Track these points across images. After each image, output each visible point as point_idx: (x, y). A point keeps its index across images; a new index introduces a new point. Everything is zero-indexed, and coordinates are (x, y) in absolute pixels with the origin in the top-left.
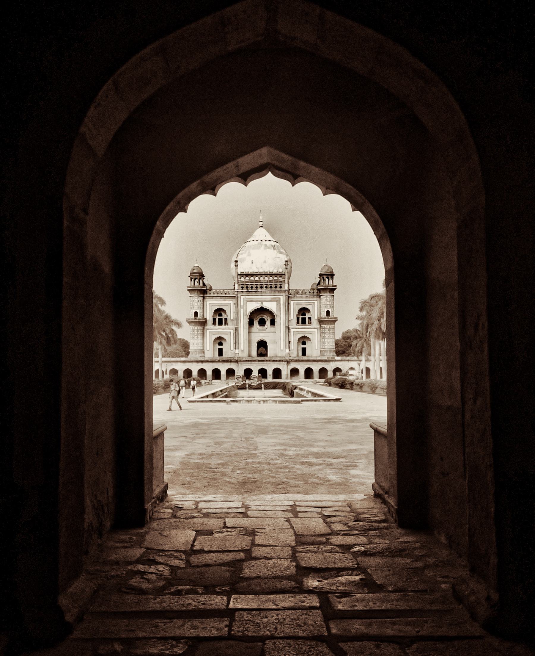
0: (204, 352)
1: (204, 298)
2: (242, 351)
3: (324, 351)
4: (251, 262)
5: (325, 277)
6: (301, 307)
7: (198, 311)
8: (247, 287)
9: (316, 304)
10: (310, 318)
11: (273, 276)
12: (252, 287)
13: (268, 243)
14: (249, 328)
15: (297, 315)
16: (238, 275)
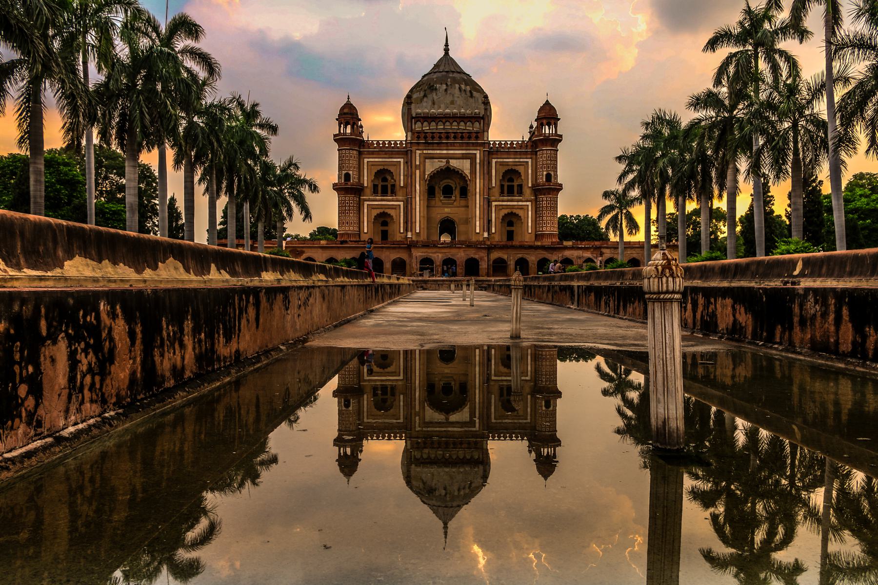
0: (359, 235)
1: (360, 153)
2: (418, 234)
3: (543, 236)
4: (430, 103)
5: (545, 122)
6: (506, 168)
7: (351, 172)
8: (425, 138)
9: (530, 164)
10: (520, 187)
11: (466, 120)
12: (433, 138)
13: (455, 75)
14: (428, 200)
15: (501, 181)
16: (413, 118)
